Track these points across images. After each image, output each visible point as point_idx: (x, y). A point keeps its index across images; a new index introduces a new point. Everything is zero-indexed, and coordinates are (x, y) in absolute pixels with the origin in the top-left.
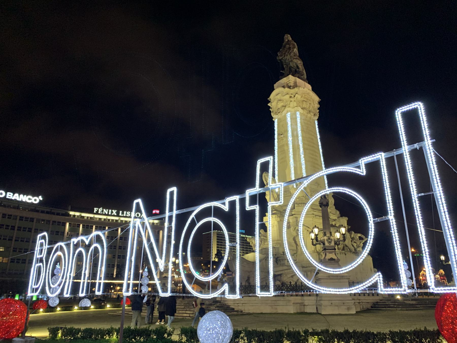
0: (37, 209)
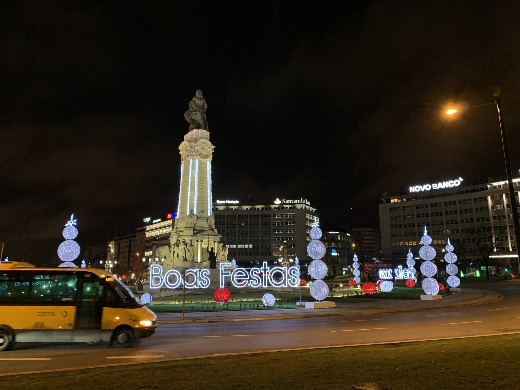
0: (461, 190)
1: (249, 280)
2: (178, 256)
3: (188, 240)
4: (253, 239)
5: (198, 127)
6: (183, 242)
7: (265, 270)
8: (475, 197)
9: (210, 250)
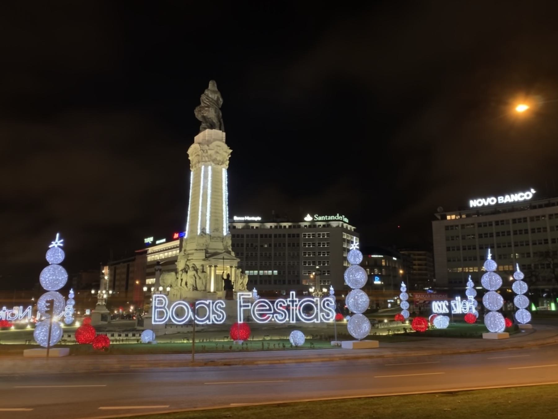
0: (534, 204)
1: (273, 314)
2: (186, 284)
3: (198, 265)
4: (278, 264)
5: (212, 127)
6: (193, 267)
7: (293, 301)
8: (551, 213)
9: (225, 277)
